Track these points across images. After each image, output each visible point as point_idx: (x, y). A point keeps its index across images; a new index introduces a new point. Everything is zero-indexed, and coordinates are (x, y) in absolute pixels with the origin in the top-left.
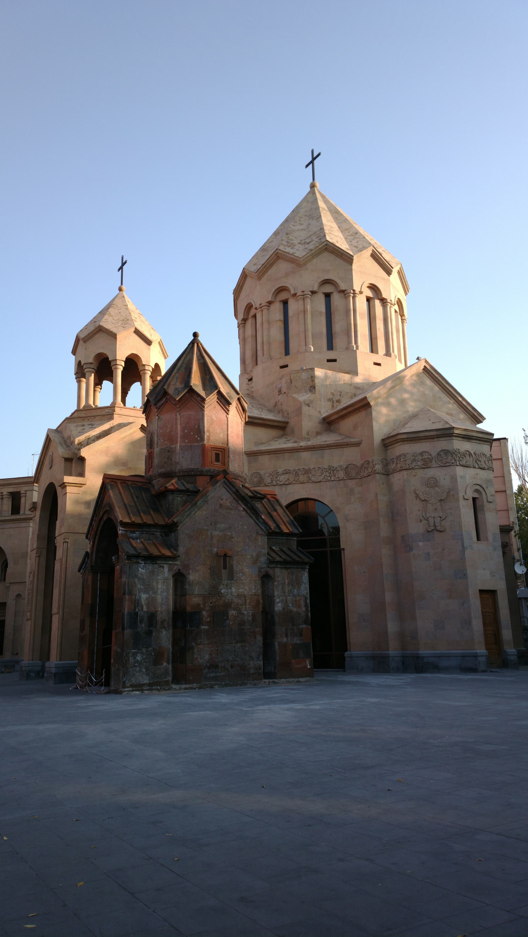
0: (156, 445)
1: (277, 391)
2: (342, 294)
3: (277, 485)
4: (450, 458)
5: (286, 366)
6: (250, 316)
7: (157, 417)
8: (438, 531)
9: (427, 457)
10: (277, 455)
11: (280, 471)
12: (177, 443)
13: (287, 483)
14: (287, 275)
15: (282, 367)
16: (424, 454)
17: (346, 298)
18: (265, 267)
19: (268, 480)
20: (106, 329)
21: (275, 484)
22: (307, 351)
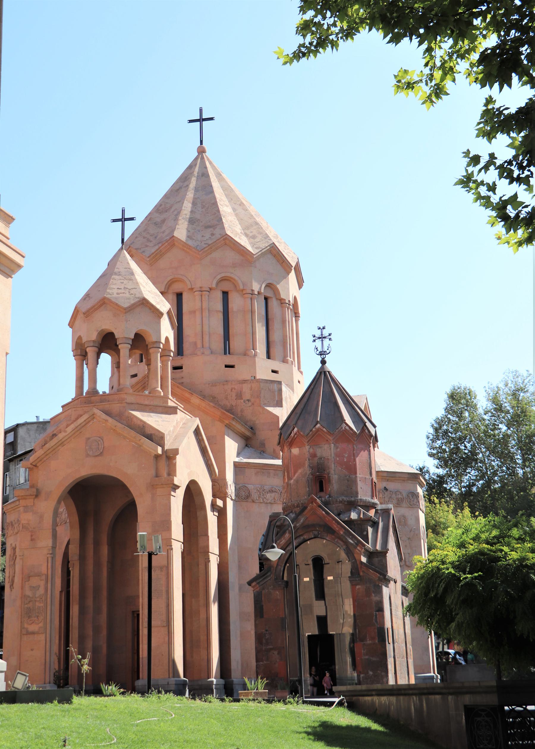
0: (332, 472)
1: (234, 394)
2: (279, 302)
3: (264, 502)
4: (416, 500)
5: (232, 367)
6: (171, 291)
7: (332, 445)
8: (407, 566)
9: (400, 496)
10: (262, 470)
11: (267, 488)
12: (356, 473)
13: (273, 502)
14: (234, 266)
15: (226, 366)
16: (397, 493)
17: (282, 307)
18: (211, 248)
19: (255, 496)
20: (152, 306)
21: (262, 501)
22: (255, 355)
